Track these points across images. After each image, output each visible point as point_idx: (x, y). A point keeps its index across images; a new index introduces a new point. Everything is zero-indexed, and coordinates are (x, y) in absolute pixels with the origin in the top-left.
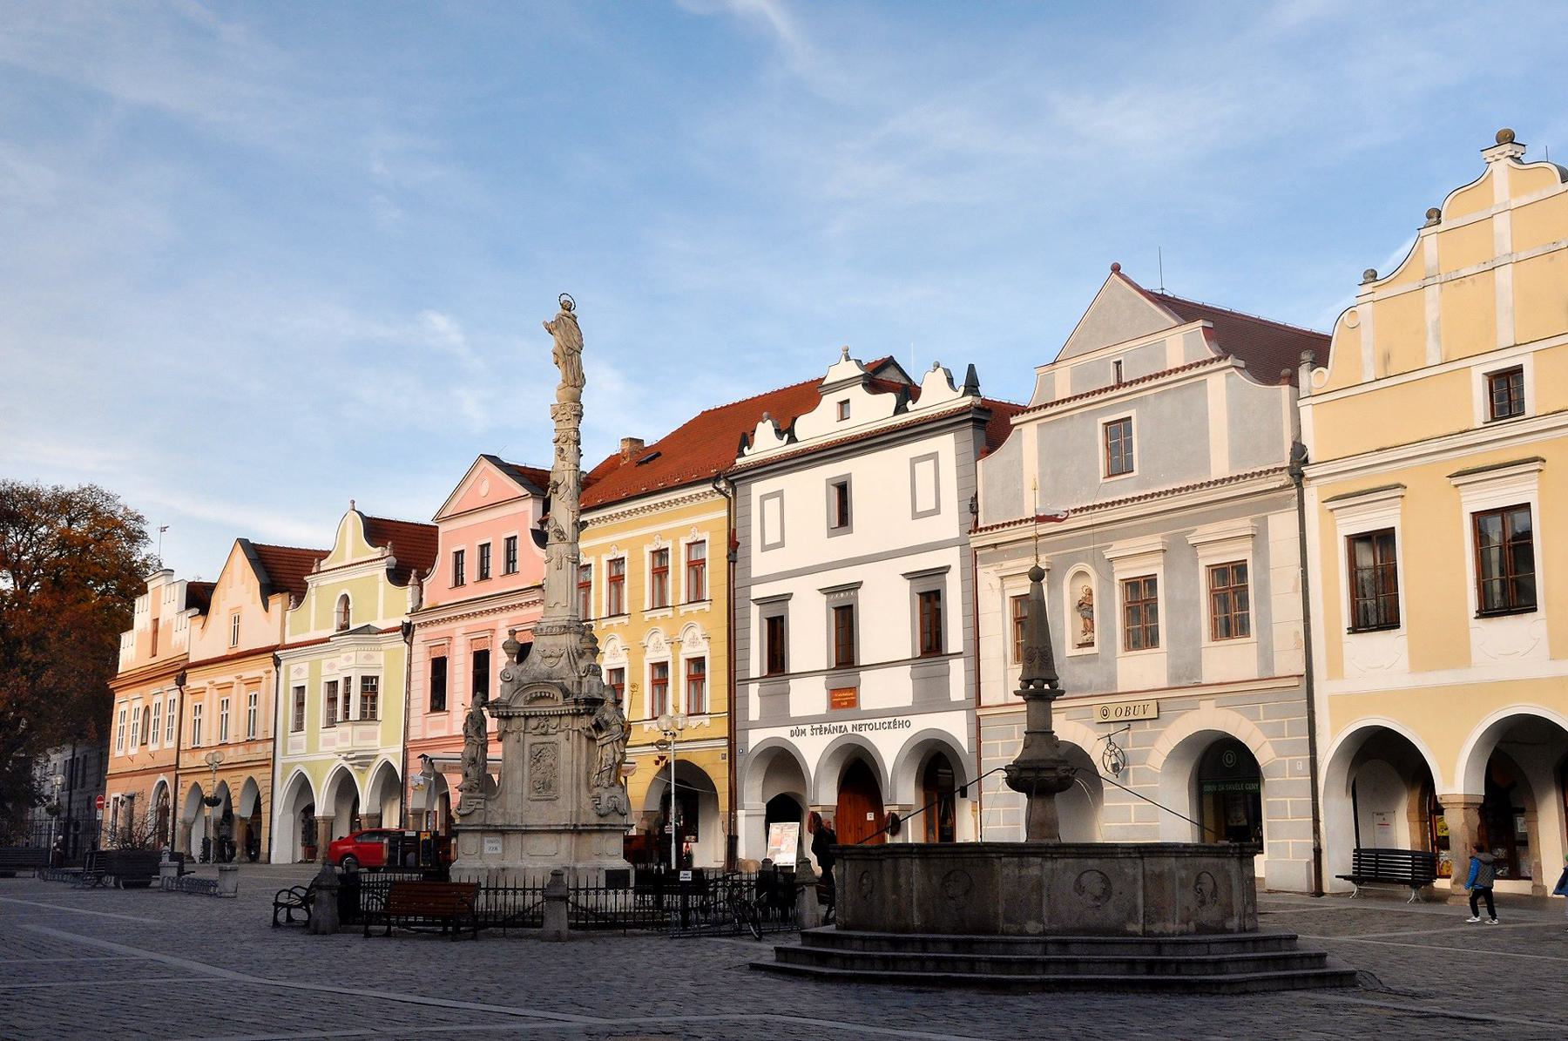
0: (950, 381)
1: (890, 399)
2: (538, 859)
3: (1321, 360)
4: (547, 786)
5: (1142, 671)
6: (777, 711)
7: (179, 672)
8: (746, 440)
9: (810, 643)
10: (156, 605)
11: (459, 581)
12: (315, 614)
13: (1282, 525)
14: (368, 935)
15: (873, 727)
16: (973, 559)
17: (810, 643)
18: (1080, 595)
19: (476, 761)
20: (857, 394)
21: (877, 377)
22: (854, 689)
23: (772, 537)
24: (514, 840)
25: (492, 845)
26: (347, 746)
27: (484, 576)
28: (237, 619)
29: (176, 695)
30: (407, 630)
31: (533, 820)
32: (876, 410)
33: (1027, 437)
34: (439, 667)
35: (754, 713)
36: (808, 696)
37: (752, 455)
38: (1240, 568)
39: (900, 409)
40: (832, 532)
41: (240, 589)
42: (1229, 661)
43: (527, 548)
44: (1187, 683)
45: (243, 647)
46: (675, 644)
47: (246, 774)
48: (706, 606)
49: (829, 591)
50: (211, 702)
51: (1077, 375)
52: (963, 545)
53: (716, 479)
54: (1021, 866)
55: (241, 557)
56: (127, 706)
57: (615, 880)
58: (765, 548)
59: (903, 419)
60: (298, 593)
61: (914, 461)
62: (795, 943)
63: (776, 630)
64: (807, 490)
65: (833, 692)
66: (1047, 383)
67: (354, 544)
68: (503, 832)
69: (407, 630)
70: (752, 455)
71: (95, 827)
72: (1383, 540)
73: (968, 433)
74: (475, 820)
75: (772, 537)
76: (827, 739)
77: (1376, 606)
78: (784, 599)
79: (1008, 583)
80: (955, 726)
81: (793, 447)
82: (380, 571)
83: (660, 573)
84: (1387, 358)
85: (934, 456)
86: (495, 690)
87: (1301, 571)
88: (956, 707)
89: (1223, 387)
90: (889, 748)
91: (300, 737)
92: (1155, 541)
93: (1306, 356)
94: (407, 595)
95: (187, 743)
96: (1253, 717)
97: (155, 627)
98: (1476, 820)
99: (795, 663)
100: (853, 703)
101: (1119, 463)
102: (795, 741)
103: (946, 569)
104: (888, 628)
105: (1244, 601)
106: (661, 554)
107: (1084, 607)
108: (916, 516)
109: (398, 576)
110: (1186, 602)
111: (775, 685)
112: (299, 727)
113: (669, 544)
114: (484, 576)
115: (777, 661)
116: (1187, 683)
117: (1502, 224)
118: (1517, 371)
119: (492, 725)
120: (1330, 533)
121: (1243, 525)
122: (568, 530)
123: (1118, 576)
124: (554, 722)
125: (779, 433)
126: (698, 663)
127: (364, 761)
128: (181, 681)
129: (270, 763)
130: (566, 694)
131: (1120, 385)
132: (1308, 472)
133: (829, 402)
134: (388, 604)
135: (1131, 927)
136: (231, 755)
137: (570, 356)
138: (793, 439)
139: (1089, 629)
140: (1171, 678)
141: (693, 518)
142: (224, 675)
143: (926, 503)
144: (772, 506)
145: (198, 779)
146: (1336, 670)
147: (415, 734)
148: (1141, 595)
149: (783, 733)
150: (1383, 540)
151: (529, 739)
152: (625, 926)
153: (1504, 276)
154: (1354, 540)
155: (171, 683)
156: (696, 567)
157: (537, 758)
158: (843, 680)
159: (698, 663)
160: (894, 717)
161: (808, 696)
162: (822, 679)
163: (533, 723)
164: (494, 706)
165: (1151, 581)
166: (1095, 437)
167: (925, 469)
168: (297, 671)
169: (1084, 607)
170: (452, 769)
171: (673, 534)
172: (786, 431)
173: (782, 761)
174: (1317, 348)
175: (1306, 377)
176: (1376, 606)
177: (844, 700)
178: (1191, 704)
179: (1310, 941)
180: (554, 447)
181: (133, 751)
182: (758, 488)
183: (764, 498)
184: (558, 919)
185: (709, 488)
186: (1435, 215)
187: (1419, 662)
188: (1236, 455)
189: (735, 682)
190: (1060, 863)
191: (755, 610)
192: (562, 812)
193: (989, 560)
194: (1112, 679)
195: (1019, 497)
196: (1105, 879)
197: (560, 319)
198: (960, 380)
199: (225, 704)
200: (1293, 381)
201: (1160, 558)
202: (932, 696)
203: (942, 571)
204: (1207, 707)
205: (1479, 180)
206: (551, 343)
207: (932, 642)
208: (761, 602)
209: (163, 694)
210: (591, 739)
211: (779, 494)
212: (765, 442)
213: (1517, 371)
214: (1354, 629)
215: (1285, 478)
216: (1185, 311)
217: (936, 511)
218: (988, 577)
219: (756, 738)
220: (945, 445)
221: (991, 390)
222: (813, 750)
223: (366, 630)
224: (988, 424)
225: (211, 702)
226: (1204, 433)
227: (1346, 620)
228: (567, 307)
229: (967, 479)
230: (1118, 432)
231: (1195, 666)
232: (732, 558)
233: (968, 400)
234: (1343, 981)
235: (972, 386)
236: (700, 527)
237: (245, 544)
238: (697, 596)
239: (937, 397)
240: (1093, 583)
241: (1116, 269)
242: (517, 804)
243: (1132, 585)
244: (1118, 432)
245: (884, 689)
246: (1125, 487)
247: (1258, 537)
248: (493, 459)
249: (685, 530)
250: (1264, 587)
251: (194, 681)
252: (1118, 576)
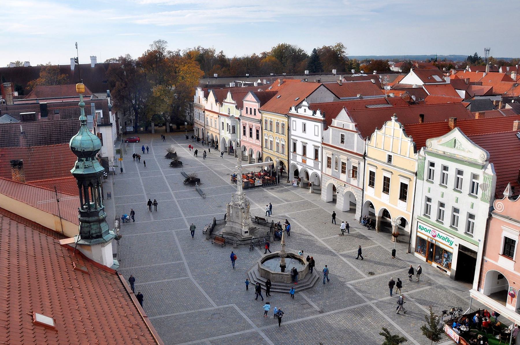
6: (295, 159)
9: (299, 150)
17: (299, 150)
24: (234, 224)
57: (246, 232)
63: (295, 145)
75: (294, 129)
88: (319, 170)
104: (310, 153)
111: (294, 155)
115: (295, 150)
149: (296, 163)
158: (304, 158)
161: (299, 159)
167: (316, 127)
207: (316, 157)
222: (300, 168)
247: (359, 164)
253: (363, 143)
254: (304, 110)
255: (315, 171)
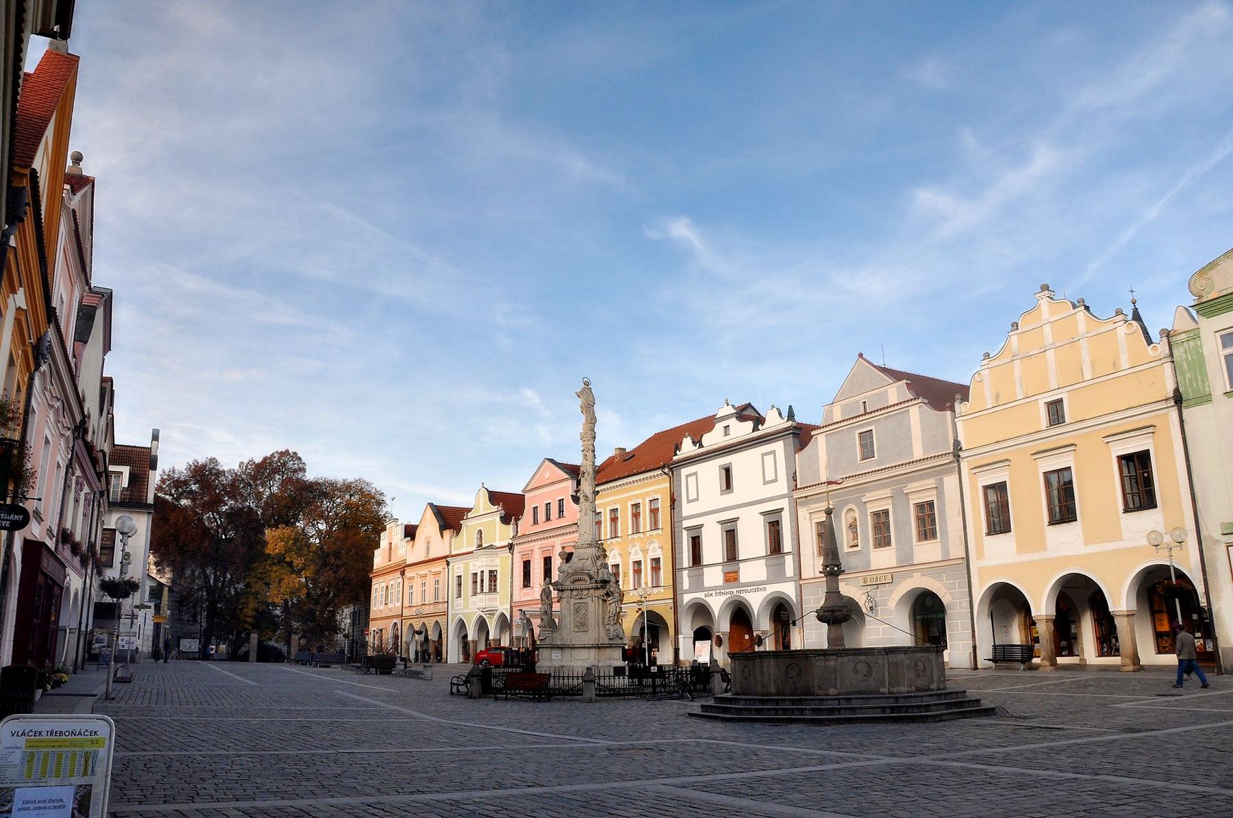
0: (780, 414)
1: (750, 424)
2: (579, 662)
3: (965, 398)
4: (583, 624)
5: (883, 558)
6: (698, 584)
7: (402, 569)
8: (678, 447)
9: (713, 549)
10: (391, 536)
11: (535, 522)
12: (465, 540)
13: (950, 482)
14: (496, 699)
15: (747, 592)
16: (795, 504)
17: (713, 549)
18: (851, 521)
19: (547, 614)
20: (733, 422)
21: (745, 413)
22: (737, 572)
23: (692, 496)
24: (567, 652)
25: (556, 655)
26: (482, 605)
27: (548, 519)
28: (428, 543)
29: (400, 580)
30: (511, 547)
31: (576, 642)
32: (743, 430)
33: (820, 442)
34: (527, 565)
35: (686, 586)
36: (713, 576)
37: (680, 455)
38: (931, 504)
39: (755, 429)
40: (723, 493)
41: (429, 527)
42: (927, 552)
43: (569, 504)
44: (906, 564)
45: (431, 557)
46: (645, 551)
47: (435, 619)
48: (660, 532)
49: (722, 523)
50: (417, 583)
51: (844, 409)
52: (789, 496)
53: (663, 467)
54: (826, 661)
55: (430, 512)
56: (378, 586)
57: (619, 671)
58: (689, 501)
59: (757, 434)
60: (457, 529)
61: (763, 455)
62: (711, 703)
63: (696, 543)
64: (710, 472)
65: (726, 574)
66: (829, 413)
67: (484, 505)
68: (561, 648)
69: (511, 547)
70: (680, 455)
71: (365, 645)
72: (1001, 488)
73: (790, 439)
74: (547, 642)
75: (692, 496)
76: (725, 597)
77: (999, 522)
78: (700, 527)
79: (813, 516)
80: (788, 590)
81: (701, 450)
82: (498, 519)
83: (636, 515)
84: (997, 396)
85: (774, 452)
86: (555, 577)
87: (961, 503)
89: (918, 414)
90: (756, 601)
91: (460, 600)
92: (887, 492)
93: (958, 396)
94: (510, 529)
95: (406, 604)
96: (940, 580)
97: (390, 548)
98: (1052, 627)
99: (706, 560)
100: (736, 579)
101: (867, 453)
102: (707, 599)
103: (780, 510)
104: (753, 540)
105: (933, 522)
106: (636, 506)
107: (853, 527)
108: (765, 483)
109: (505, 520)
110: (905, 523)
111: (695, 571)
112: (459, 596)
113: (640, 501)
114: (548, 519)
115: (697, 559)
116: (906, 564)
117: (1047, 329)
118: (1060, 401)
119: (554, 594)
120: (975, 484)
121: (931, 482)
122: (590, 495)
123: (869, 511)
124: (585, 592)
125: (694, 443)
126: (657, 560)
127: (491, 613)
128: (403, 574)
129: (446, 614)
130: (591, 578)
131: (866, 413)
132: (962, 454)
133: (719, 427)
134: (501, 534)
135: (882, 690)
136: (427, 610)
137: (589, 408)
138: (701, 446)
139: (855, 538)
140: (898, 562)
141: (652, 487)
142: (423, 570)
143: (770, 476)
144: (692, 480)
145: (412, 621)
146: (981, 555)
147: (516, 599)
148: (881, 520)
149: (701, 595)
150: (1001, 488)
151: (573, 601)
152: (624, 695)
153: (1083, 343)
154: (986, 488)
155: (398, 574)
156: (654, 512)
157: (577, 611)
158: (731, 568)
159: (657, 560)
160: (757, 585)
161: (713, 576)
162: (763, 561)
163: (575, 593)
164: (555, 584)
165: (886, 512)
166: (854, 441)
168: (458, 567)
169: (853, 527)
170: (535, 616)
171: (643, 496)
172: (697, 442)
173: (701, 610)
174: (962, 392)
175: (958, 407)
176: (999, 522)
177: (731, 577)
178: (908, 575)
179: (972, 693)
180: (581, 454)
181: (381, 608)
182: (685, 471)
183: (687, 476)
184: (590, 692)
185: (660, 472)
186: (1015, 326)
187: (1021, 549)
188: (925, 448)
189: (675, 570)
190: (845, 659)
191: (685, 533)
192: (590, 638)
193: (803, 504)
194: (869, 564)
195: (817, 471)
196: (869, 666)
197: (583, 390)
198: (785, 413)
199: (424, 584)
200: (952, 409)
201: (890, 501)
202: (777, 574)
203: (780, 510)
204: (917, 575)
205: (1035, 308)
206: (579, 402)
207: (776, 547)
208: (687, 529)
209: (394, 580)
210: (604, 601)
211: (695, 474)
212: (688, 448)
213: (1060, 401)
214: (989, 534)
215: (951, 458)
216: (896, 375)
217: (775, 480)
218: (803, 513)
219: (687, 598)
220: (779, 446)
221: (800, 418)
222: (717, 604)
223: (491, 547)
224: (800, 435)
225: (417, 583)
226: (910, 437)
227: (985, 530)
228: (587, 384)
229: (790, 463)
230: (866, 436)
231: (911, 554)
232: (672, 507)
233: (790, 423)
234: (989, 712)
235: (791, 416)
236: (655, 492)
237: (431, 505)
238: (655, 527)
239: (774, 422)
240: (857, 515)
241: (861, 355)
242: (569, 634)
243: (876, 515)
244: (866, 436)
245: (753, 571)
246: (870, 465)
247: (939, 489)
248: (551, 461)
249: (648, 494)
250: (943, 513)
251: (408, 574)
252: (869, 511)
253: (944, 420)
254: (722, 430)
255: (773, 589)
